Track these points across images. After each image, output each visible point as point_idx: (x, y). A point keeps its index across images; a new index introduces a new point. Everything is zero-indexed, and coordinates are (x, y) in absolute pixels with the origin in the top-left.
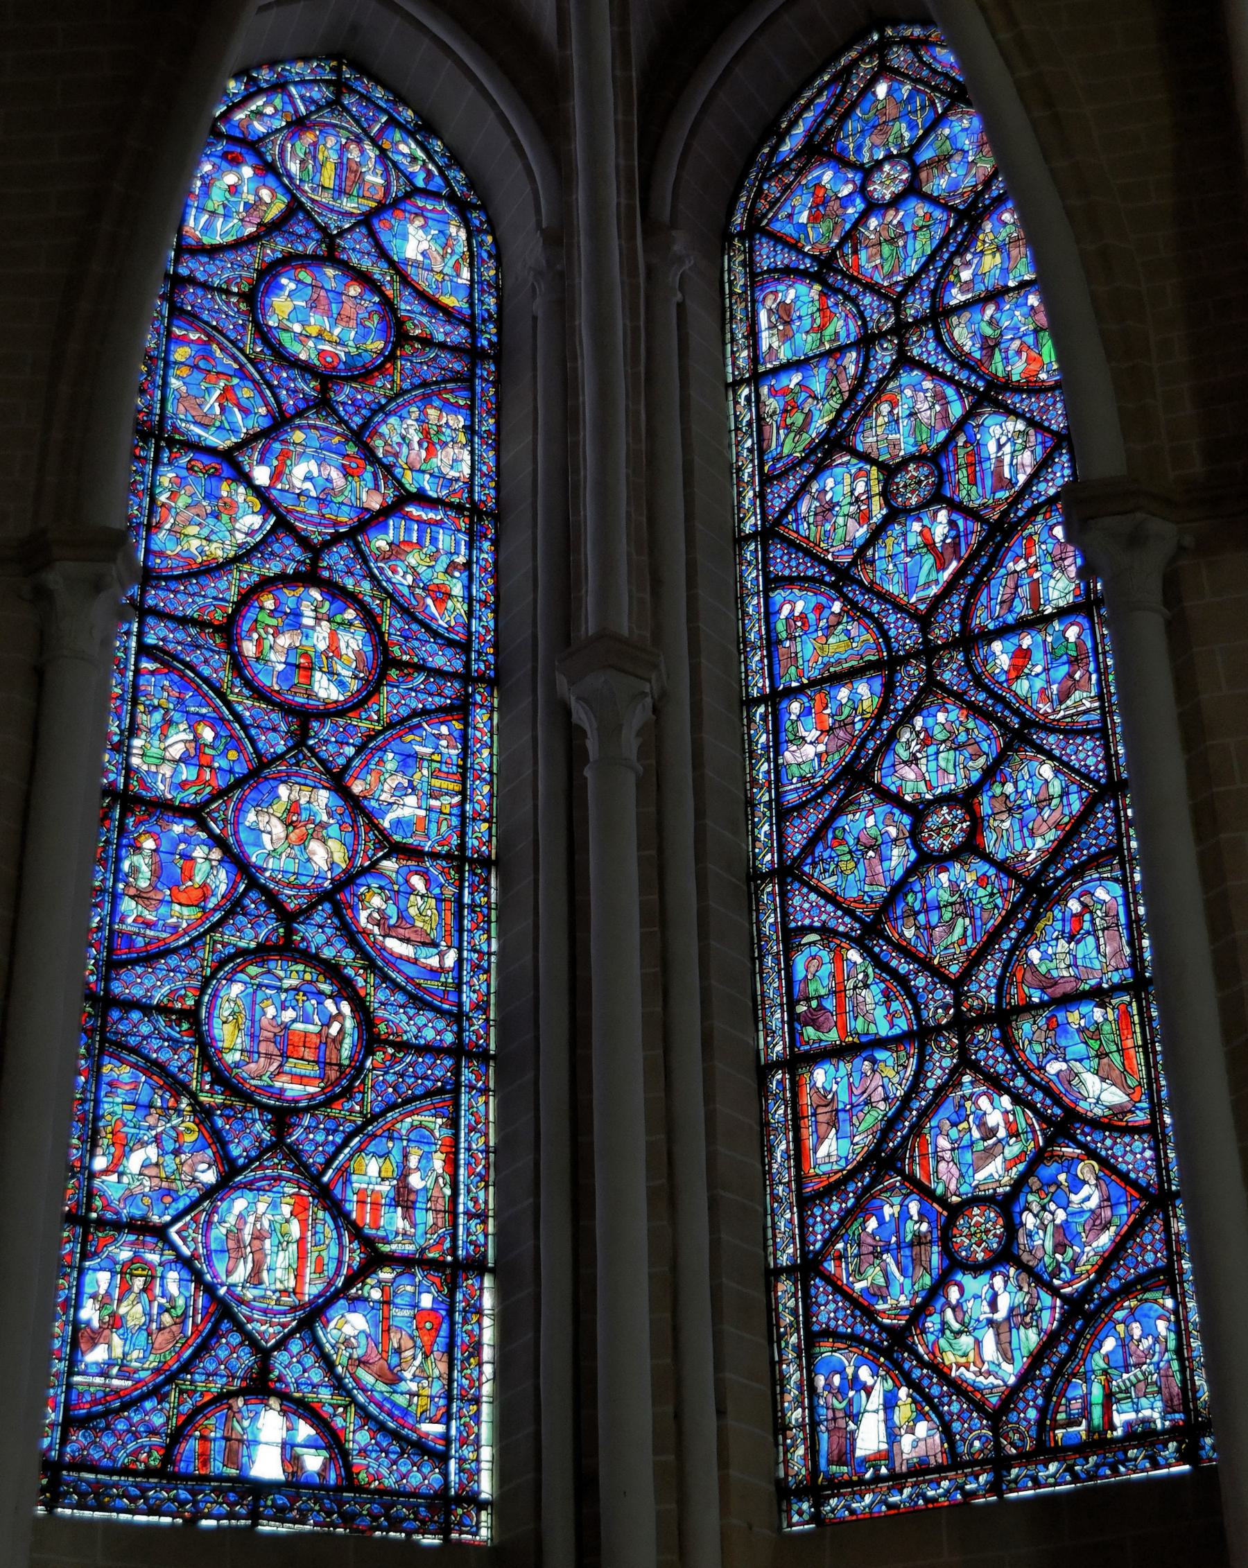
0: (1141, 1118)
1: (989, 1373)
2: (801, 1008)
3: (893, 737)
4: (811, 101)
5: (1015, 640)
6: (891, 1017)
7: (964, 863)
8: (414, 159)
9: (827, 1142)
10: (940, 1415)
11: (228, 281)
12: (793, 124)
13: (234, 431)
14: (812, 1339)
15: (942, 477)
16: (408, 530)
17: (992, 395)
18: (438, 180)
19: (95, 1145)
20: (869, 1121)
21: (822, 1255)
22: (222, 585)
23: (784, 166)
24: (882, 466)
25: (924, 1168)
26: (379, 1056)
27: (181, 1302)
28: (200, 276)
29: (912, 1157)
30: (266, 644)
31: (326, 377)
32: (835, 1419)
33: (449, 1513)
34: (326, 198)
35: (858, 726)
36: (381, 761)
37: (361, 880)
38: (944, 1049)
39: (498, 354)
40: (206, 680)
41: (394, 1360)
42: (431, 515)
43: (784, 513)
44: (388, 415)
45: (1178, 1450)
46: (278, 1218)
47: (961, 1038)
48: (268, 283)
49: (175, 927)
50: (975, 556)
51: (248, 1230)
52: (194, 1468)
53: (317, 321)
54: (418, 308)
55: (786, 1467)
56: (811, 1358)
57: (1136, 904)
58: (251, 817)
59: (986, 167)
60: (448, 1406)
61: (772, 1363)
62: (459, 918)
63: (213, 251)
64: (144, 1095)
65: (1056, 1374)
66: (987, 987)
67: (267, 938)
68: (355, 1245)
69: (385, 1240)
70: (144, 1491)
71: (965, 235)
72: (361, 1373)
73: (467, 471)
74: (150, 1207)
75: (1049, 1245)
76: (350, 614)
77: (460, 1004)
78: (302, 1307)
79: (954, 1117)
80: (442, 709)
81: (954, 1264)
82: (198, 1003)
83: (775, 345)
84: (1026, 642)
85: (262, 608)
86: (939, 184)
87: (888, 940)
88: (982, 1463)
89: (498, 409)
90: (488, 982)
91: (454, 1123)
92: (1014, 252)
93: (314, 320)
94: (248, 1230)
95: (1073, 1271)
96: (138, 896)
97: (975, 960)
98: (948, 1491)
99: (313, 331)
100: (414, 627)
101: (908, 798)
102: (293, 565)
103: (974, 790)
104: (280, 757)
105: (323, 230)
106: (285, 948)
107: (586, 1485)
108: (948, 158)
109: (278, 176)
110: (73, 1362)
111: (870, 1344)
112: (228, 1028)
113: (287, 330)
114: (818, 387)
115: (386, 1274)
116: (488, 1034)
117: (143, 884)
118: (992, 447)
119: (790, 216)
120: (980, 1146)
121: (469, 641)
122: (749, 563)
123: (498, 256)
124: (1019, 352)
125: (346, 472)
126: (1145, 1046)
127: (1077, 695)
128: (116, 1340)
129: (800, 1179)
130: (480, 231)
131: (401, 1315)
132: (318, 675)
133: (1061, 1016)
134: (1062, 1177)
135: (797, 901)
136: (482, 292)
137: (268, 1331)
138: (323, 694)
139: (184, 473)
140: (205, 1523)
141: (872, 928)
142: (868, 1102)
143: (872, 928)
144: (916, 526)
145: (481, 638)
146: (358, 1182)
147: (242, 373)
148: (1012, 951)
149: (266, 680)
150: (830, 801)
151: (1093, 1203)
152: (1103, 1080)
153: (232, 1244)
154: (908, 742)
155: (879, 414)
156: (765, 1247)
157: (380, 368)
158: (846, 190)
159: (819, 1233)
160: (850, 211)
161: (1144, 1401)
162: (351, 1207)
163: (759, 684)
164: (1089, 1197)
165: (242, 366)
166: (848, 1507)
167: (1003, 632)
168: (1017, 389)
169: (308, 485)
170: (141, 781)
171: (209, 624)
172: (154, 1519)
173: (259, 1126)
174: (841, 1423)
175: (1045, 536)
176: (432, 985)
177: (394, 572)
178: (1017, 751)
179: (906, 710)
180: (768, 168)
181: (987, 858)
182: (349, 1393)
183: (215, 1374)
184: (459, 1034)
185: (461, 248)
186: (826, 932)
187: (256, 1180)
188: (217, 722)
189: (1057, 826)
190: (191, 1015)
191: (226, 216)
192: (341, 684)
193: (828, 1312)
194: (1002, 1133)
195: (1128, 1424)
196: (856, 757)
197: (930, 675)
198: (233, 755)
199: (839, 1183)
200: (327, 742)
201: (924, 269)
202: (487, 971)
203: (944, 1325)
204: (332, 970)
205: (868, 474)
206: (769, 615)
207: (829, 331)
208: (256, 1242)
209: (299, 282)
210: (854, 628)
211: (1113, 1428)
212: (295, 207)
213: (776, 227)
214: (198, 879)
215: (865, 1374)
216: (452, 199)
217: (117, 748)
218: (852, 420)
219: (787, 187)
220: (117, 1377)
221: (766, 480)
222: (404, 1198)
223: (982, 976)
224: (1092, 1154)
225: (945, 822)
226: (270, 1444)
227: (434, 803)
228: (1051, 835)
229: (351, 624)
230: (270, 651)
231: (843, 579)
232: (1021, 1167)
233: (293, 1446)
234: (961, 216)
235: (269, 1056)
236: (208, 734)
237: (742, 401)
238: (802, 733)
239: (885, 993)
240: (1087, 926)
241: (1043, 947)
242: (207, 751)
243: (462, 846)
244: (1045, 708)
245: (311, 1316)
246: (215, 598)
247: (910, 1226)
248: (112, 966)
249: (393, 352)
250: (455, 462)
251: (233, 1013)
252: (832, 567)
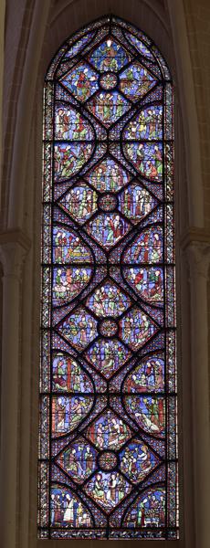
0: (162, 436)
3: (93, 292)
12: (74, 44)
17: (138, 179)
20: (76, 419)
24: (97, 192)
56: (50, 489)
75: (130, 468)
81: (99, 468)
84: (142, 272)
86: (127, 91)
88: (103, 529)
97: (115, 375)
103: (120, 318)
119: (71, 81)
124: (149, 166)
129: (50, 432)
141: (80, 355)
143: (80, 355)
144: (108, 219)
150: (70, 308)
151: (145, 459)
154: (99, 295)
158: (93, 79)
164: (144, 456)
167: (135, 266)
180: (63, 58)
181: (122, 342)
186: (65, 353)
189: (146, 337)
196: (80, 295)
201: (118, 122)
203: (95, 486)
207: (83, 133)
213: (65, 83)
215: (68, 496)
218: (88, 171)
219: (70, 69)
221: (55, 184)
224: (146, 444)
231: (80, 229)
239: (85, 379)
244: (146, 296)
252: (77, 224)
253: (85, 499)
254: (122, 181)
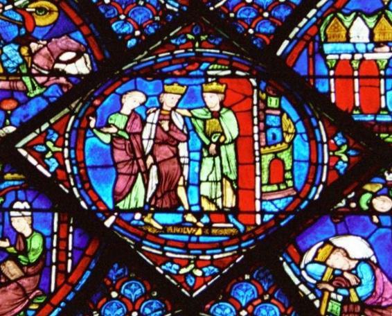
27: (36, 243)
46: (200, 113)
51: (148, 131)
68: (339, 140)
94: (148, 131)
153: (120, 155)
208: (164, 152)
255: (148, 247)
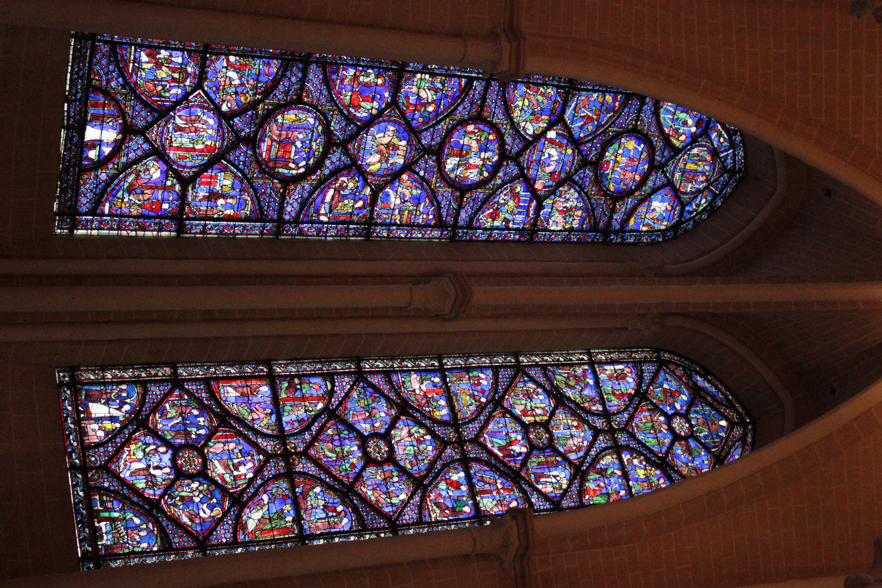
0: (241, 537)
1: (126, 465)
2: (296, 381)
4: (720, 390)
5: (465, 482)
6: (291, 422)
7: (362, 457)
8: (698, 206)
9: (234, 392)
10: (107, 442)
11: (642, 120)
12: (709, 382)
13: (572, 123)
14: (144, 384)
15: (542, 450)
16: (525, 201)
17: (579, 473)
18: (688, 216)
19: (240, 56)
20: (243, 411)
21: (182, 389)
22: (501, 116)
23: (690, 377)
24: (548, 422)
25: (221, 437)
26: (279, 186)
27: (167, 94)
28: (645, 108)
29: (226, 431)
30: (472, 136)
31: (598, 164)
32: (106, 393)
33: (68, 216)
34: (681, 165)
35: (427, 409)
36: (417, 188)
37: (361, 178)
38: (275, 446)
39: (607, 243)
40: (456, 108)
41: (138, 191)
42: (532, 212)
43: (528, 375)
44: (579, 193)
45: (88, 551)
47: (280, 455)
48: (641, 138)
49: (340, 93)
50: (505, 464)
51: (200, 125)
52: (91, 100)
53: (623, 160)
54: (629, 207)
55: (85, 370)
57: (340, 537)
58: (392, 128)
59: (685, 471)
60: (116, 216)
61: (133, 365)
62: (343, 223)
63: (656, 114)
64: (263, 78)
65: (124, 495)
66: (303, 467)
67: (335, 135)
68: (191, 174)
69: (194, 188)
70: (81, 78)
71: (654, 461)
72: (133, 176)
73: (552, 228)
74: (211, 81)
75: (183, 494)
76: (486, 174)
77: (303, 223)
78: (164, 149)
79: (244, 451)
80: (441, 215)
82: (305, 103)
83: (607, 372)
84: (464, 488)
85: (489, 134)
86: (678, 450)
87: (327, 422)
88: (85, 462)
89: (581, 243)
90: (313, 236)
91: (247, 219)
92: (645, 484)
93: (624, 159)
94: (200, 125)
95: (171, 504)
96: (355, 77)
97: (316, 462)
98: (72, 445)
99: (619, 159)
100: (479, 204)
101: (393, 432)
102: (509, 148)
103: (396, 463)
104: (419, 142)
105: (666, 164)
106: (330, 143)
107: (79, 280)
108: (690, 454)
109: (691, 144)
110: (141, 46)
111: (141, 409)
112: (293, 117)
113: (619, 147)
114: (586, 392)
115: (178, 188)
116: (289, 235)
117: (361, 79)
118: (555, 473)
119: (667, 380)
120: (230, 463)
121: (472, 229)
122: (505, 359)
123: (653, 243)
124: (598, 486)
125: (552, 173)
126: (274, 540)
127: (438, 511)
128: (150, 66)
129: (217, 379)
130: (664, 235)
131: (159, 194)
132: (458, 159)
133: (289, 501)
134: (214, 501)
135: (347, 379)
136: (636, 236)
137: (153, 135)
138: (449, 161)
139: (553, 99)
140: (66, 105)
141: (333, 414)
142: (252, 411)
143: (333, 414)
144: (519, 438)
145: (474, 234)
146: (221, 175)
147: (599, 126)
148: (320, 479)
149: (456, 135)
150: (393, 396)
151: (202, 514)
152: (259, 520)
153: (193, 118)
154: (419, 432)
155: (573, 420)
156: (186, 362)
157: (601, 189)
158: (678, 406)
159: (192, 387)
160: (668, 408)
161: (110, 536)
162: (209, 173)
163: (449, 363)
164: (205, 513)
165: (603, 126)
166: (66, 399)
167: (469, 477)
168: (581, 485)
169: (547, 156)
170: (408, 79)
171: (482, 110)
172: (68, 82)
173: (247, 130)
174: (104, 396)
175: (513, 497)
176: (312, 210)
177: (505, 195)
178: (413, 483)
179: (434, 431)
180: (690, 370)
181: (363, 469)
182: (123, 171)
183: (134, 109)
184: (288, 222)
185: (656, 227)
187: (223, 129)
188: (436, 113)
189: (378, 501)
190: (300, 100)
191: (673, 120)
192: (453, 170)
193: (156, 391)
194: (236, 473)
195: (101, 529)
196: (413, 408)
197: (449, 443)
198: (421, 120)
199: (215, 397)
200: (426, 163)
202: (317, 235)
203: (148, 445)
204: (319, 164)
205: (545, 415)
206: (481, 368)
207: (613, 398)
209: (642, 153)
210: (473, 408)
211: (99, 522)
212: (676, 151)
213: (662, 373)
214: (363, 104)
215: (127, 408)
216: (679, 223)
217: (425, 67)
218: (570, 408)
219: (680, 378)
220: (134, 65)
221: (544, 368)
222: (213, 196)
223: (309, 465)
224: (225, 514)
225: (381, 449)
226: (101, 135)
227: (397, 212)
228: (373, 498)
229: (481, 174)
230: (470, 138)
231: (496, 403)
232: (220, 482)
233: (100, 145)
234: (663, 460)
235: (280, 135)
236: (431, 109)
237: (581, 357)
238: (425, 383)
239: (302, 420)
240: (330, 514)
241: (321, 494)
242: (423, 109)
243: (376, 224)
244: (433, 496)
245: (159, 153)
246: (494, 113)
247: (194, 430)
248: (323, 64)
249: (609, 195)
250: (557, 223)
251: (300, 119)
252: (502, 398)
253: (127, 432)
254: (570, 452)
255: (163, 123)
